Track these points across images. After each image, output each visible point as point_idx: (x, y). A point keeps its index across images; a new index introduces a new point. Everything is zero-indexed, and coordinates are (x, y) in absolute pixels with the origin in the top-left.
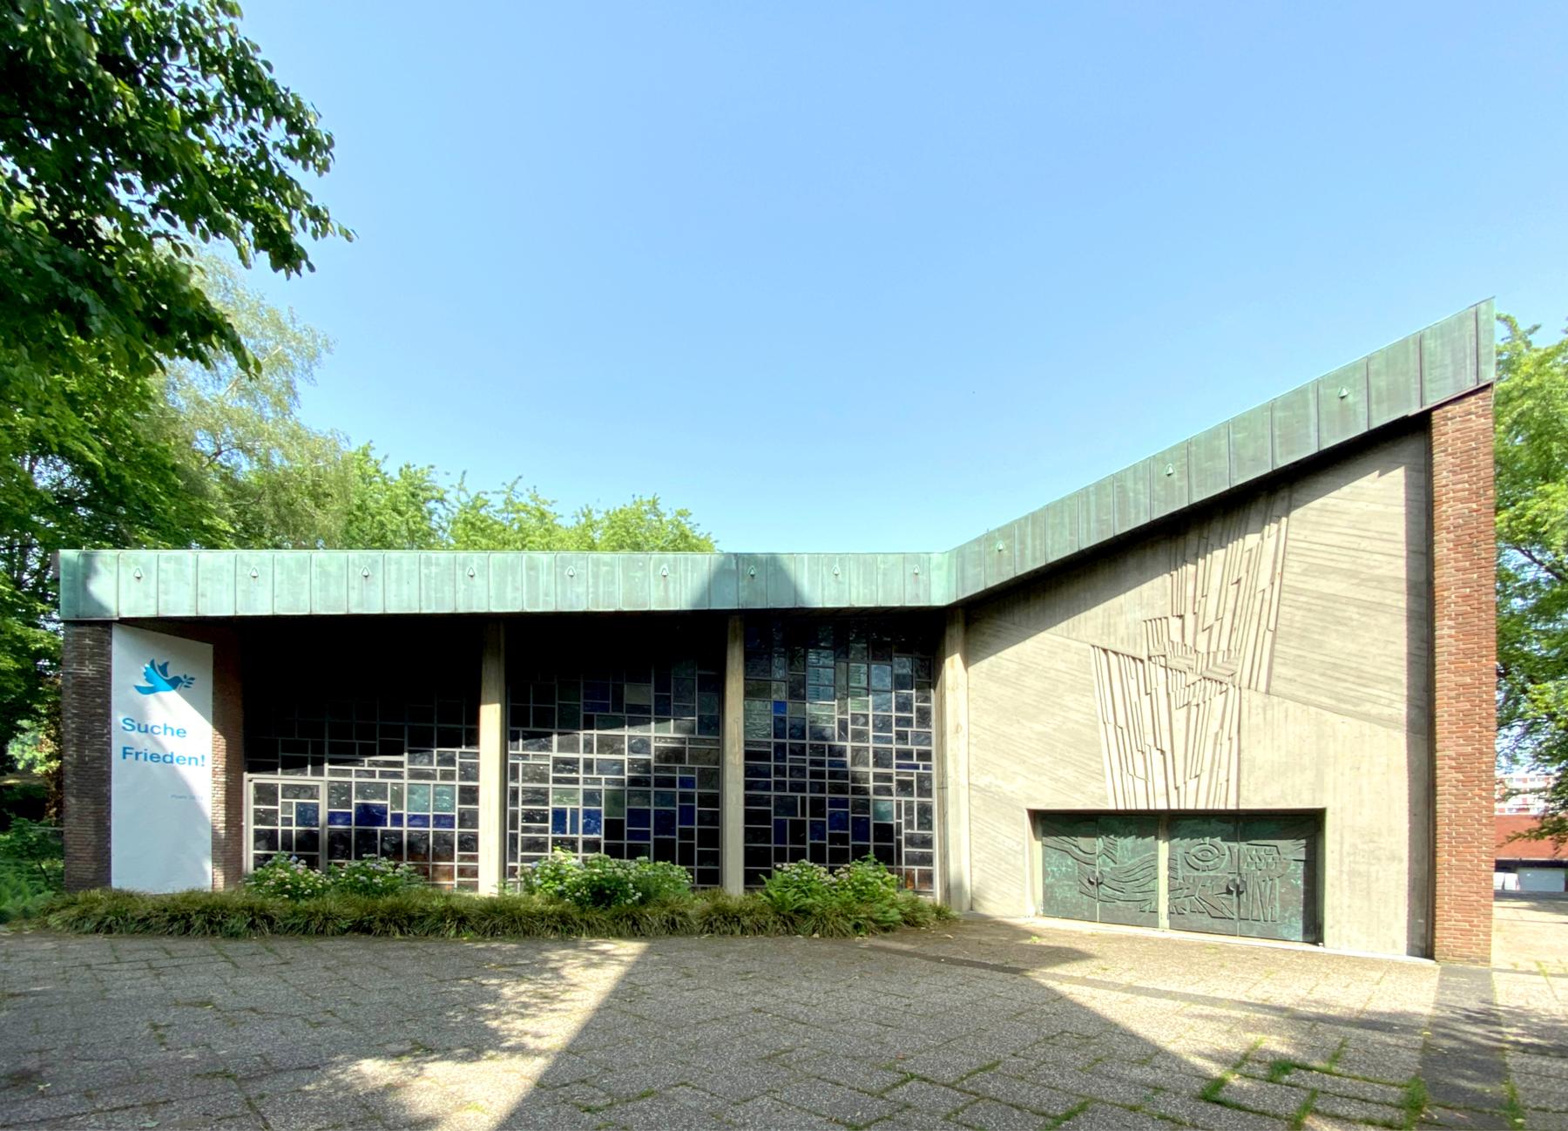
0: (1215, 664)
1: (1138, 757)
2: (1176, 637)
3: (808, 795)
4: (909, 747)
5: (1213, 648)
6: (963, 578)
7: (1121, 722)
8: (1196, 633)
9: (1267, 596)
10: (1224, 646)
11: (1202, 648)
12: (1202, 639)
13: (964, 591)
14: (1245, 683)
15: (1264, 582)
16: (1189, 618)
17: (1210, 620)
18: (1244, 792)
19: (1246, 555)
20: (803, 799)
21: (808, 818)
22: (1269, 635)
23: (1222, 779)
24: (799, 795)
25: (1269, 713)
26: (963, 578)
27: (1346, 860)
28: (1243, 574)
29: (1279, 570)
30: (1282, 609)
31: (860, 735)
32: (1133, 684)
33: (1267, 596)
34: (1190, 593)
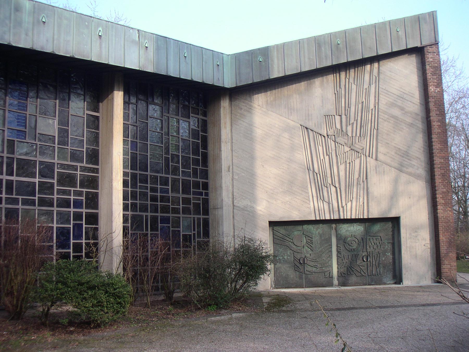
0: (355, 143)
1: (325, 189)
2: (338, 126)
3: (149, 214)
4: (198, 180)
5: (354, 135)
6: (239, 74)
7: (316, 170)
8: (347, 126)
9: (373, 113)
10: (358, 135)
11: (350, 134)
12: (349, 128)
13: (240, 81)
14: (367, 154)
15: (372, 106)
16: (344, 117)
17: (352, 121)
18: (370, 210)
19: (364, 91)
20: (147, 216)
21: (149, 232)
22: (375, 131)
23: (361, 203)
24: (144, 214)
25: (378, 169)
26: (239, 74)
27: (408, 241)
28: (364, 100)
29: (377, 101)
30: (380, 120)
31: (175, 171)
32: (320, 148)
33: (373, 113)
34: (343, 105)
